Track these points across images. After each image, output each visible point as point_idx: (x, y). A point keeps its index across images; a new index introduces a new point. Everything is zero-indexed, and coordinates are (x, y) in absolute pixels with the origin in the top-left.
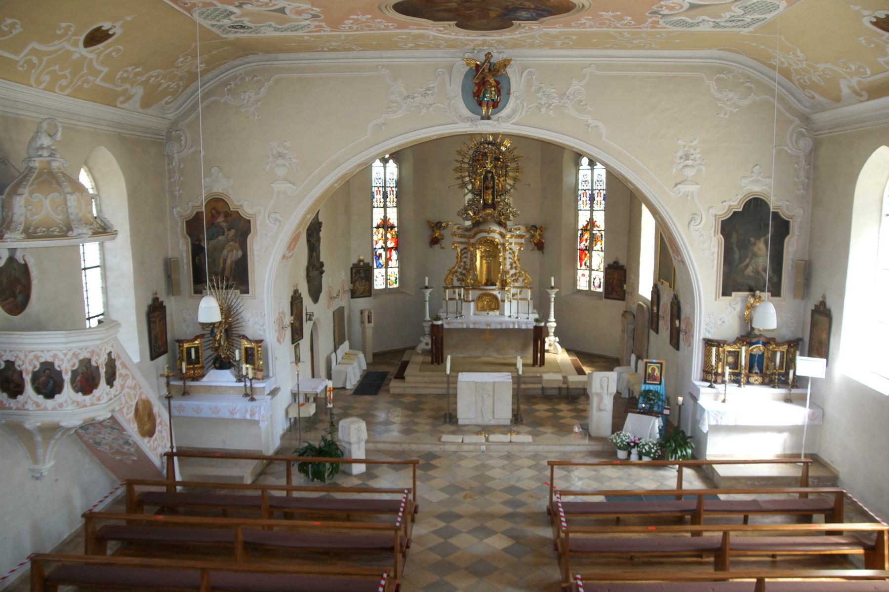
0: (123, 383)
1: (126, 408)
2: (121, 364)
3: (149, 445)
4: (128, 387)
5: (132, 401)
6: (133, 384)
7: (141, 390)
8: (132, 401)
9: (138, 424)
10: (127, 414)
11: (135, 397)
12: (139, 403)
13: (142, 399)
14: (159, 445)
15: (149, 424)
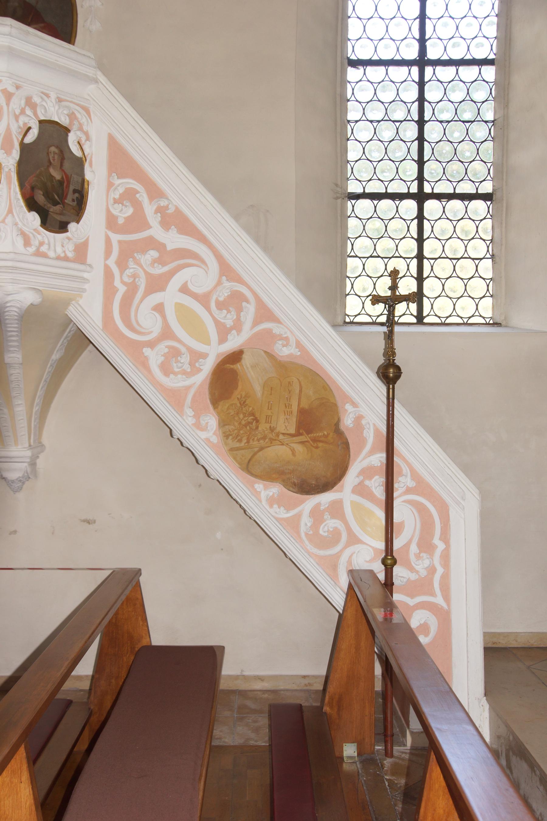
0: (159, 270)
1: (162, 347)
2: (160, 210)
3: (283, 514)
4: (184, 289)
5: (207, 342)
6: (223, 294)
7: (266, 325)
8: (207, 342)
9: (222, 423)
10: (166, 369)
11: (222, 340)
12: (247, 360)
13: (271, 356)
14: (353, 540)
15: (299, 448)
